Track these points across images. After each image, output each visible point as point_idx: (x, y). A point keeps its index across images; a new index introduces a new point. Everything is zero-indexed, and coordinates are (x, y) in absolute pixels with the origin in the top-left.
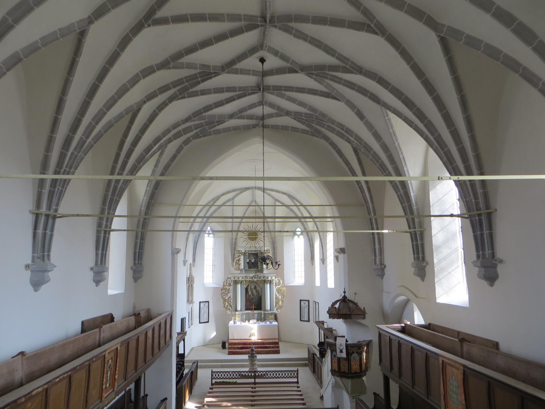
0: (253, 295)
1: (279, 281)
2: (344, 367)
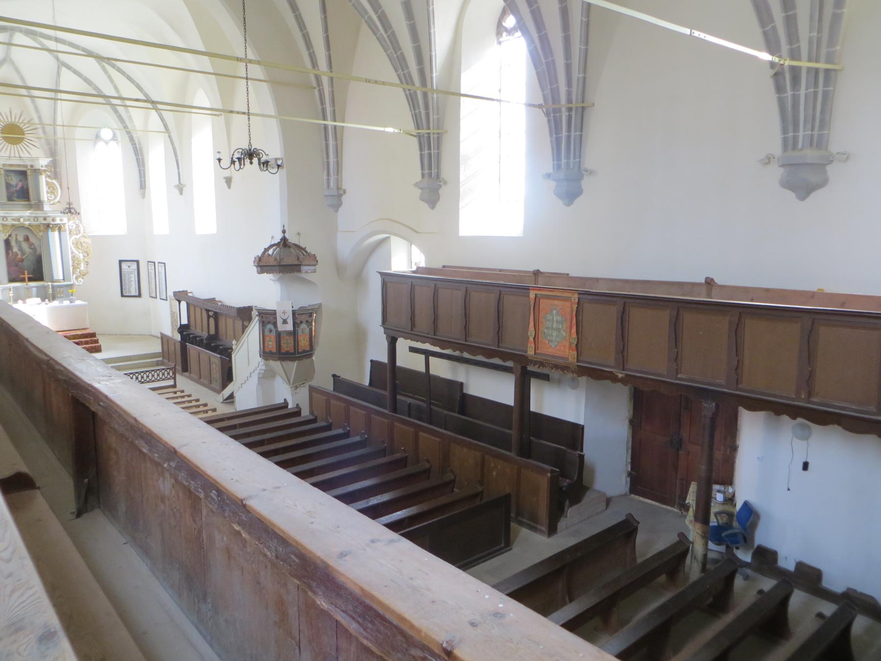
1: (77, 226)
2: (287, 345)
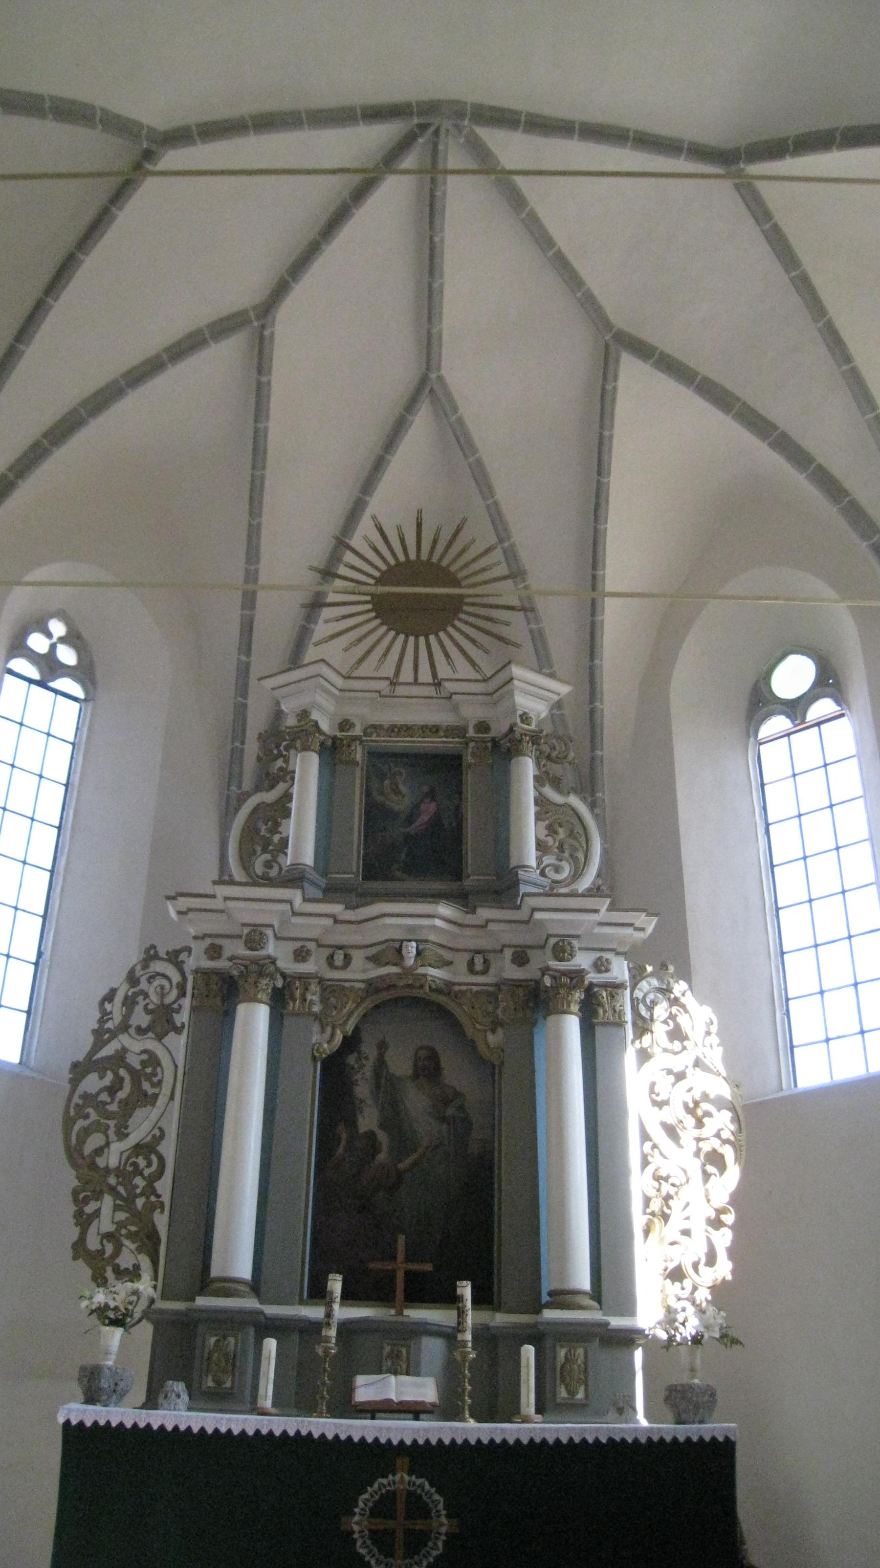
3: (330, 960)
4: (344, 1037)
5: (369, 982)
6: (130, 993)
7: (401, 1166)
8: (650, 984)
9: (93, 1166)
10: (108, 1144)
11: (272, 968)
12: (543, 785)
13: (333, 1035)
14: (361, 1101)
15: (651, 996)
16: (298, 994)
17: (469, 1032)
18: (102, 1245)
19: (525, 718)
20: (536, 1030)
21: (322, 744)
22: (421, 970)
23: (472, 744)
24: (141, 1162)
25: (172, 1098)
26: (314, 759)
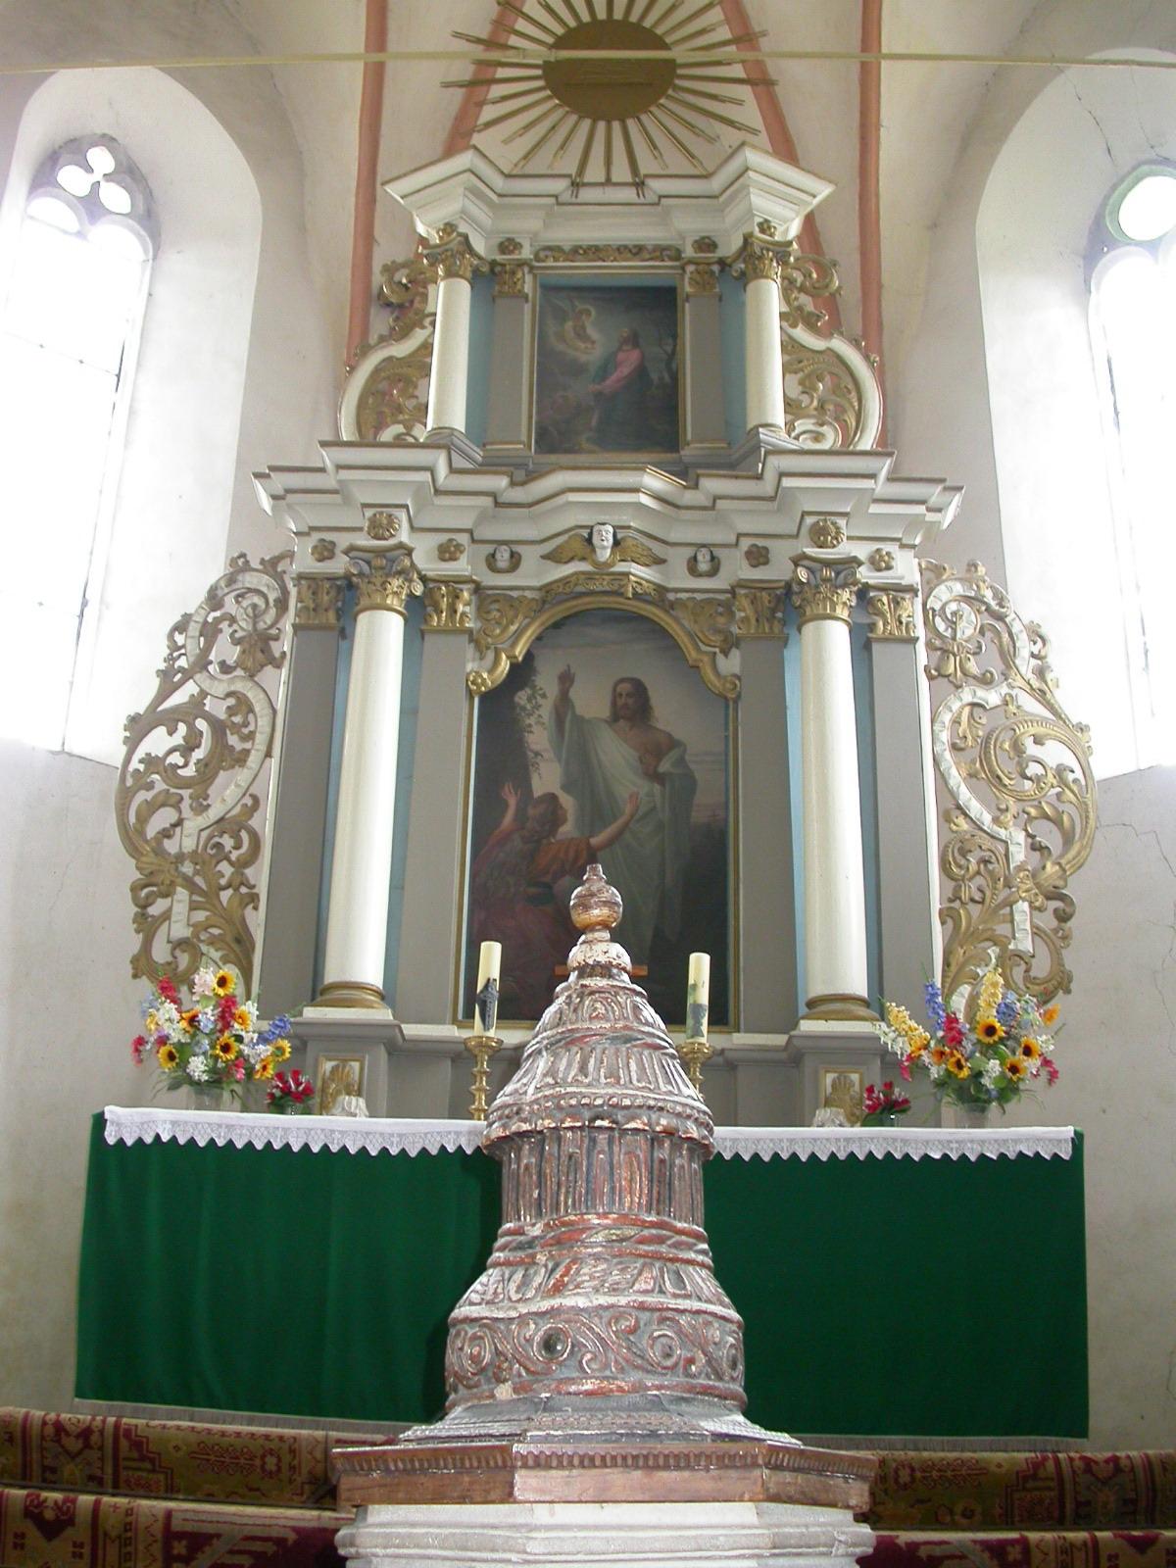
0: (597, 810)
3: (491, 561)
4: (512, 666)
5: (547, 589)
6: (210, 620)
7: (594, 841)
8: (950, 590)
9: (159, 851)
10: (179, 823)
11: (407, 562)
12: (794, 326)
13: (497, 661)
14: (537, 754)
15: (953, 607)
16: (444, 603)
17: (692, 655)
18: (175, 957)
19: (765, 227)
20: (787, 653)
21: (476, 272)
22: (621, 567)
23: (690, 268)
24: (227, 842)
25: (268, 754)
26: (464, 288)
